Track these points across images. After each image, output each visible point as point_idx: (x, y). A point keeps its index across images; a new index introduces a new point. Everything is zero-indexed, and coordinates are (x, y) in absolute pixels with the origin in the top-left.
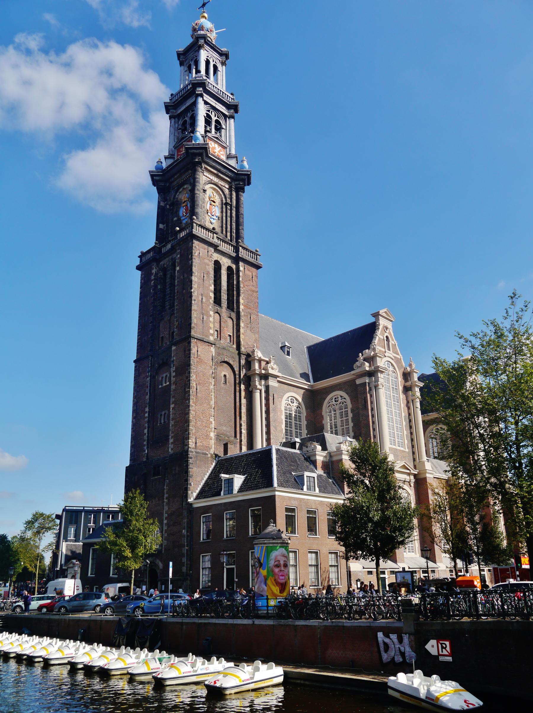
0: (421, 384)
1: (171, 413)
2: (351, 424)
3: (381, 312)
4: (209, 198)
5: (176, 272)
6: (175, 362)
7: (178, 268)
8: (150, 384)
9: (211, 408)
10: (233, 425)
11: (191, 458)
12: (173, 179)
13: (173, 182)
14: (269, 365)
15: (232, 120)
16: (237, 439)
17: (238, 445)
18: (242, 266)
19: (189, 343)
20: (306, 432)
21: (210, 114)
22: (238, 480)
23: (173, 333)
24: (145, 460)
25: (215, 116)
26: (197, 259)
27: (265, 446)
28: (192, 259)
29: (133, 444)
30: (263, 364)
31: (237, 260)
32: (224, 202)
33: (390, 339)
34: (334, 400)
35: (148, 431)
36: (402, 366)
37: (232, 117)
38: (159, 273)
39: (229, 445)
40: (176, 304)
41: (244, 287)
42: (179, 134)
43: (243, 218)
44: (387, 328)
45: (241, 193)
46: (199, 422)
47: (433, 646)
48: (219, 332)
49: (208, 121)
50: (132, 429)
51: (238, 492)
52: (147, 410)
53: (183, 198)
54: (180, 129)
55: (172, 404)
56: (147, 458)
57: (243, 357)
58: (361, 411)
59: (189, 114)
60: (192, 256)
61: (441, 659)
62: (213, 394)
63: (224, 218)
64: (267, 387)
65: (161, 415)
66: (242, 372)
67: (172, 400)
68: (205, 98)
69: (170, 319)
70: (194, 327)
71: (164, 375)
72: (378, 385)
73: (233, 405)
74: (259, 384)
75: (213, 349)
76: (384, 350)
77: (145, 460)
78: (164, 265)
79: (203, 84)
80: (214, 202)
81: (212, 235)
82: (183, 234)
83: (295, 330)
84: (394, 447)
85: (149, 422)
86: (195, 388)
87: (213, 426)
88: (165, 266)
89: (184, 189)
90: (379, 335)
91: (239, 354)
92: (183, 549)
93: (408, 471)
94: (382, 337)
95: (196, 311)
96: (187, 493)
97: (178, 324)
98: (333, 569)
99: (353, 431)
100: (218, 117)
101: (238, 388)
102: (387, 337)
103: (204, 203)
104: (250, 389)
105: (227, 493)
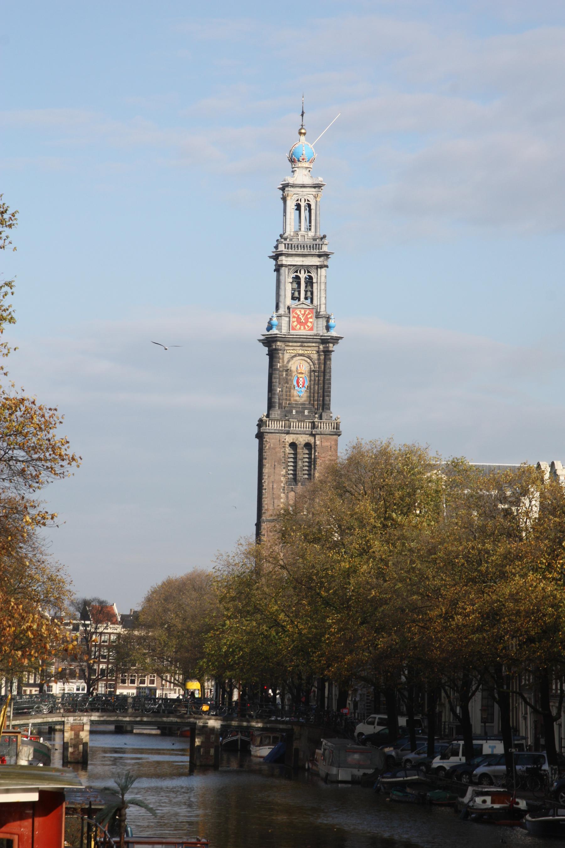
21: (298, 274)
103: (287, 383)
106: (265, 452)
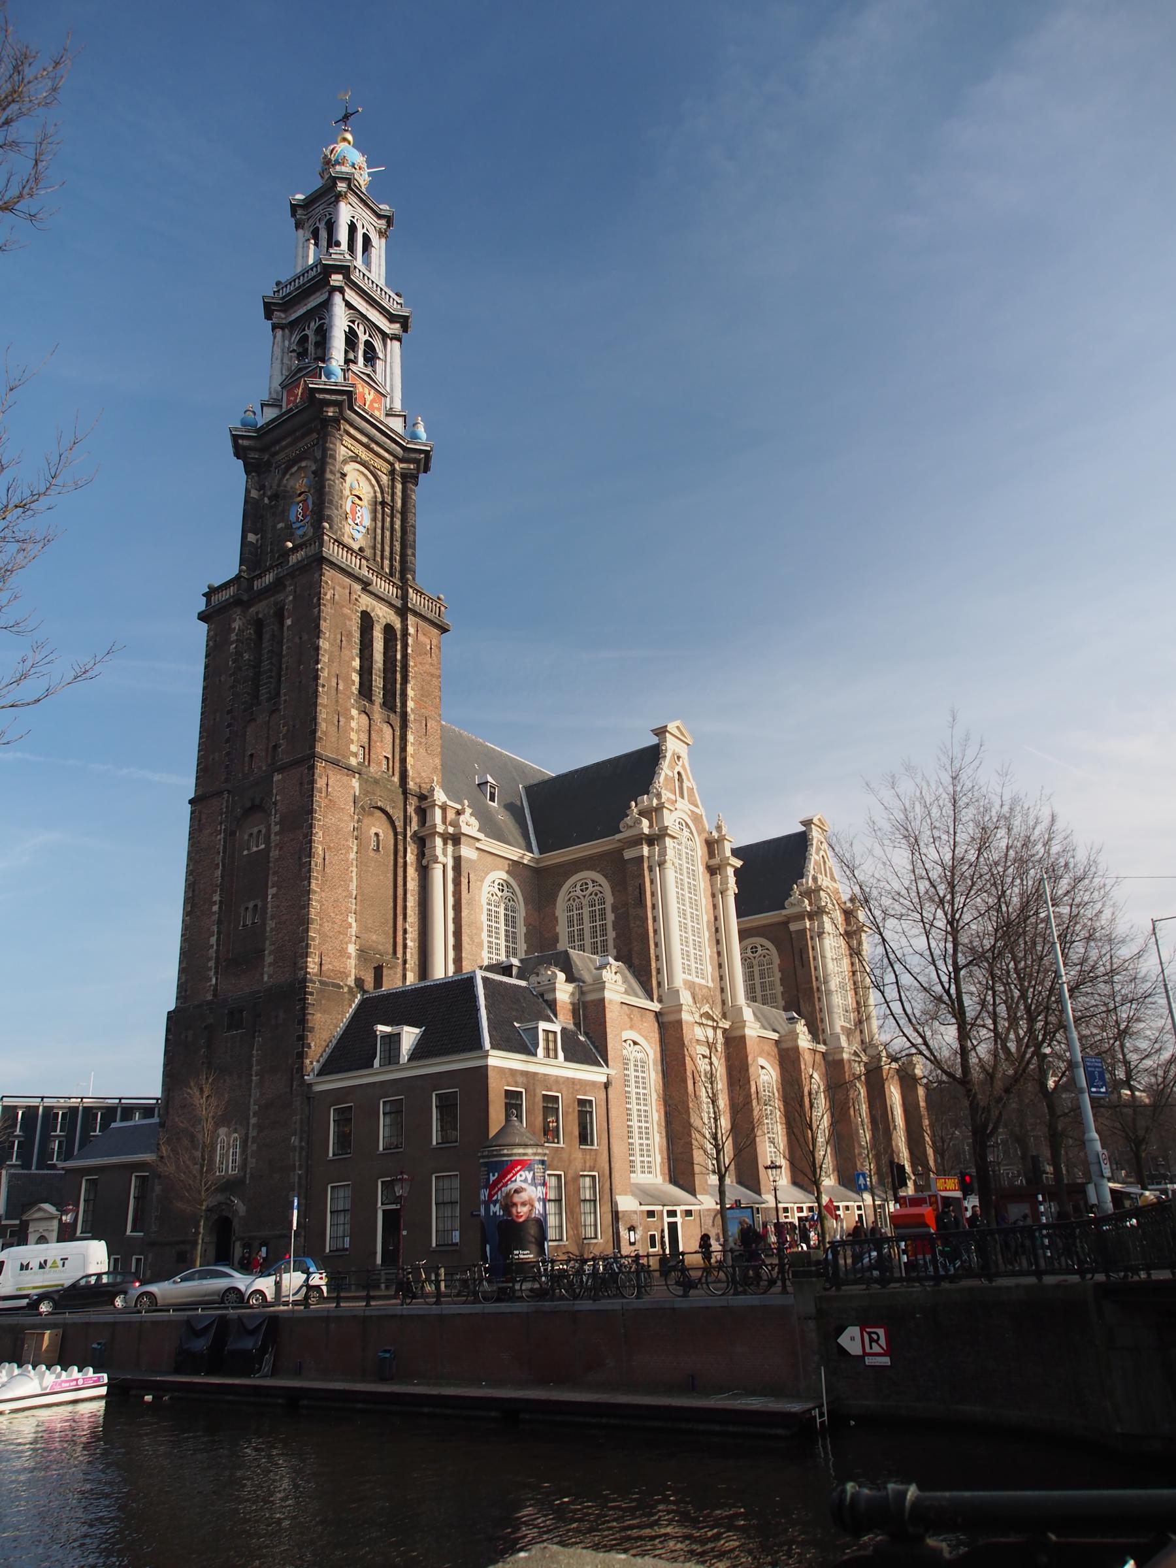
0: (738, 863)
1: (269, 905)
2: (611, 934)
3: (671, 727)
4: (351, 491)
5: (285, 628)
6: (279, 804)
7: (289, 622)
8: (225, 847)
9: (351, 897)
10: (391, 931)
11: (311, 994)
12: (277, 448)
13: (277, 453)
14: (462, 818)
15: (396, 344)
16: (398, 959)
17: (399, 969)
18: (412, 626)
19: (312, 768)
20: (524, 947)
21: (355, 327)
22: (409, 1036)
23: (275, 747)
24: (209, 997)
25: (365, 333)
26: (329, 606)
27: (450, 974)
28: (319, 605)
29: (184, 965)
30: (451, 815)
31: (403, 611)
32: (380, 499)
33: (684, 777)
34: (578, 888)
35: (218, 940)
36: (704, 830)
37: (398, 339)
38: (247, 629)
39: (384, 969)
40: (282, 692)
41: (416, 666)
42: (290, 359)
43: (414, 534)
44: (679, 758)
45: (410, 485)
46: (326, 924)
47: (853, 1339)
48: (367, 750)
49: (351, 339)
50: (182, 936)
51: (409, 1060)
52: (216, 898)
53: (297, 487)
54: (294, 351)
55: (272, 887)
56: (215, 995)
57: (413, 803)
58: (632, 911)
59: (312, 324)
60: (319, 599)
61: (869, 1361)
62: (355, 869)
63: (379, 531)
64: (458, 860)
65: (247, 909)
66: (408, 828)
67: (272, 879)
68: (347, 297)
69: (269, 721)
70: (321, 738)
71: (255, 830)
72: (665, 861)
73: (391, 892)
74: (443, 853)
75: (355, 783)
76: (673, 797)
77: (209, 997)
78: (257, 613)
79: (345, 270)
80: (360, 499)
82: (301, 554)
83: (501, 754)
84: (689, 978)
85: (219, 922)
86: (322, 856)
87: (353, 930)
88: (260, 616)
89: (300, 468)
90: (666, 770)
91: (405, 792)
92: (292, 1174)
93: (715, 1024)
94: (671, 774)
95: (325, 706)
96: (303, 1063)
97: (288, 731)
98: (587, 1207)
99: (615, 947)
100: (370, 336)
101: (400, 860)
102: (679, 773)
103: (341, 498)
104: (424, 862)
105: (387, 1062)
106: (325, 605)
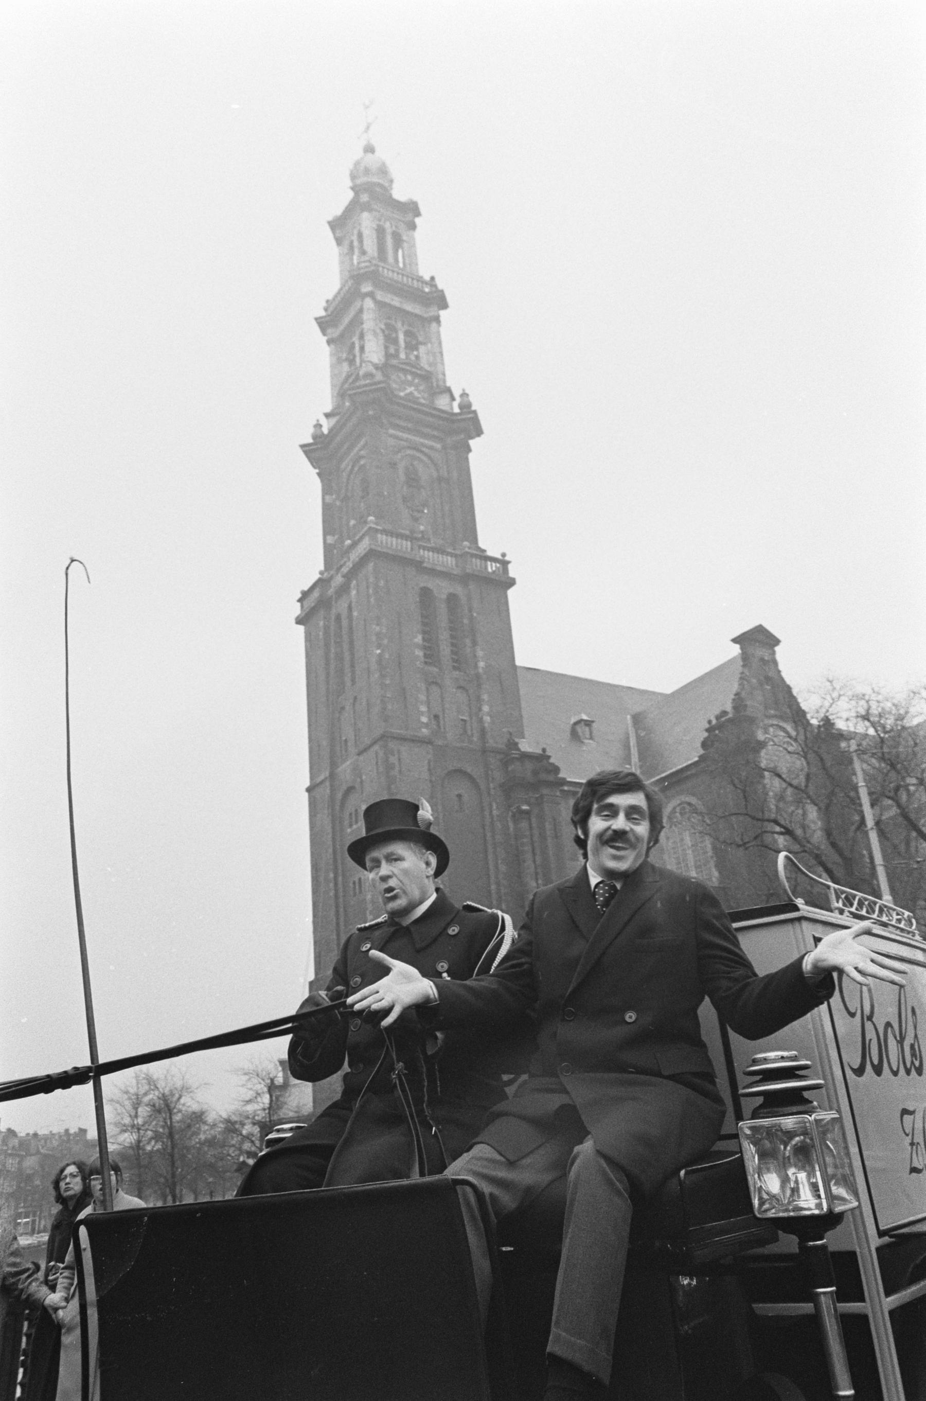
15: (434, 325)
81: (409, 543)
100: (410, 325)
